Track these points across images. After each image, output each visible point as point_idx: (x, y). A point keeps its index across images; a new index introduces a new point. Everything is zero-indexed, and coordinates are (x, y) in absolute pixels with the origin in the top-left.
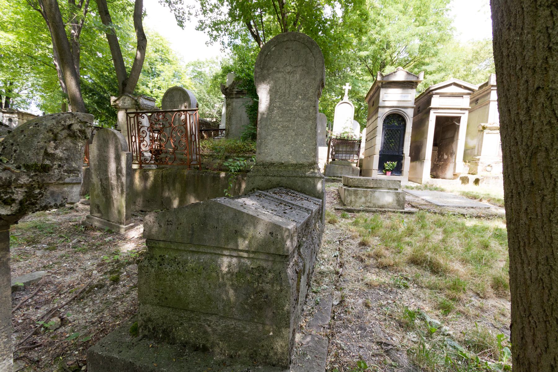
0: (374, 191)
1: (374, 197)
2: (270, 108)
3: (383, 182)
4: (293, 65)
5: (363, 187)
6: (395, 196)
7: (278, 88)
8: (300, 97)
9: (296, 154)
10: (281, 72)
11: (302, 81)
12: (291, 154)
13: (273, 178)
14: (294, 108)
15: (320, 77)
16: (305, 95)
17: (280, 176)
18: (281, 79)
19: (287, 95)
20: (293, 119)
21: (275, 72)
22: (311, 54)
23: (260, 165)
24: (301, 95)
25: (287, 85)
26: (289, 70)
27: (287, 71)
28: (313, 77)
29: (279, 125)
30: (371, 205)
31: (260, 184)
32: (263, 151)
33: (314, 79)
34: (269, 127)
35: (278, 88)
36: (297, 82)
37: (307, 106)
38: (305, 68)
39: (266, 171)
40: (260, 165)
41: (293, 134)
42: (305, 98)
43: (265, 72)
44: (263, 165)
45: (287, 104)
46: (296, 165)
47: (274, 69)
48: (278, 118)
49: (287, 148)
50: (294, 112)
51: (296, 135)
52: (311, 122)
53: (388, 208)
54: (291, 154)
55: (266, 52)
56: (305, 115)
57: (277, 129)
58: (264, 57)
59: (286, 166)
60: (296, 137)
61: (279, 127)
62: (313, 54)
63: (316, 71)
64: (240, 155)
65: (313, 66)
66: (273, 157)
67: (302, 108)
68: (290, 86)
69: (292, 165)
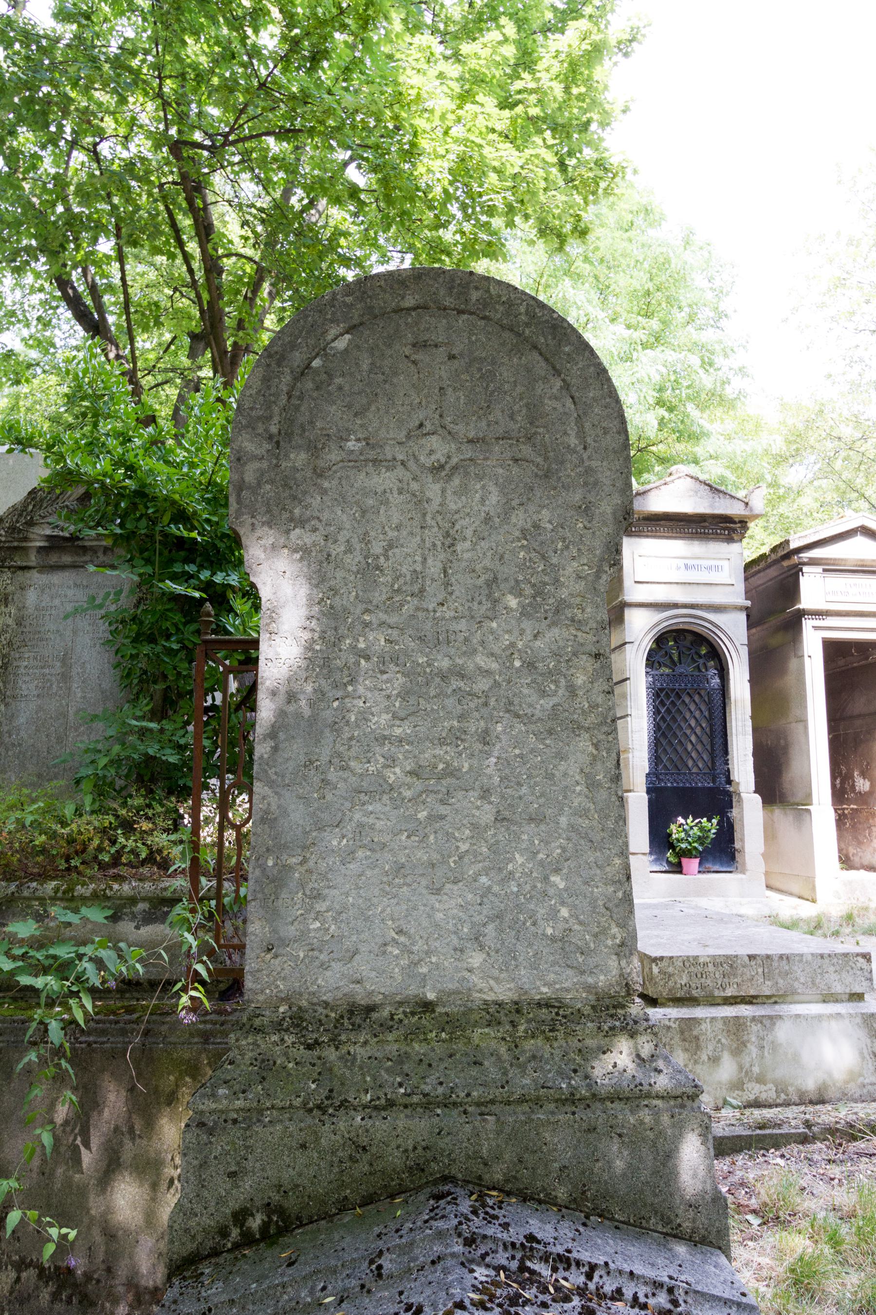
0: (773, 1019)
1: (775, 1047)
2: (326, 659)
3: (797, 969)
4: (460, 429)
5: (712, 1002)
6: (862, 1034)
7: (377, 548)
8: (513, 602)
9: (510, 937)
10: (392, 464)
11: (519, 518)
12: (477, 938)
13: (380, 1127)
14: (481, 660)
15: (617, 500)
16: (539, 592)
17: (428, 1104)
18: (396, 499)
19: (435, 592)
20: (474, 726)
21: (356, 462)
22: (559, 383)
23: (278, 1026)
24: (519, 594)
25: (433, 535)
26: (440, 456)
27: (428, 462)
28: (577, 497)
29: (391, 761)
30: (767, 1093)
31: (287, 1175)
32: (292, 931)
33: (586, 510)
34: (332, 775)
35: (377, 548)
36: (488, 519)
37: (556, 655)
38: (526, 450)
39: (325, 1072)
40: (278, 1026)
41: (486, 814)
42: (543, 605)
43: (299, 458)
44: (298, 1021)
45: (440, 640)
46: (517, 1008)
47: (351, 445)
48: (386, 717)
49: (449, 907)
50: (483, 684)
51: (499, 819)
52: (584, 744)
53: (845, 1097)
54: (477, 938)
55: (297, 358)
56: (547, 703)
57: (383, 789)
58: (287, 378)
59: (455, 1025)
60: (502, 836)
61: (394, 775)
62: (566, 386)
63: (589, 471)
64: (79, 890)
65: (573, 441)
66: (362, 966)
67: (530, 665)
68: (450, 542)
69: (496, 1014)
